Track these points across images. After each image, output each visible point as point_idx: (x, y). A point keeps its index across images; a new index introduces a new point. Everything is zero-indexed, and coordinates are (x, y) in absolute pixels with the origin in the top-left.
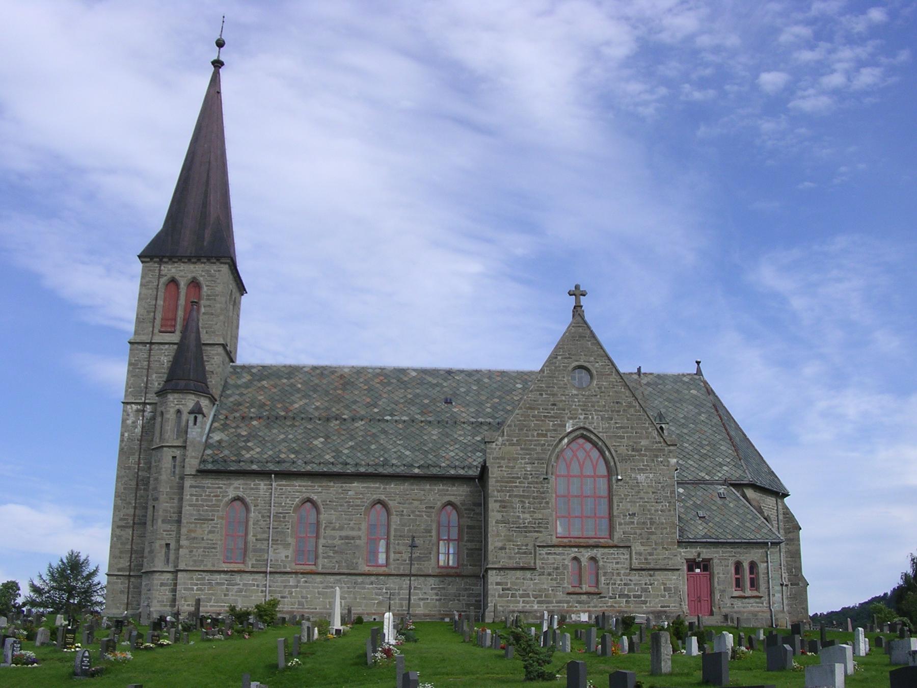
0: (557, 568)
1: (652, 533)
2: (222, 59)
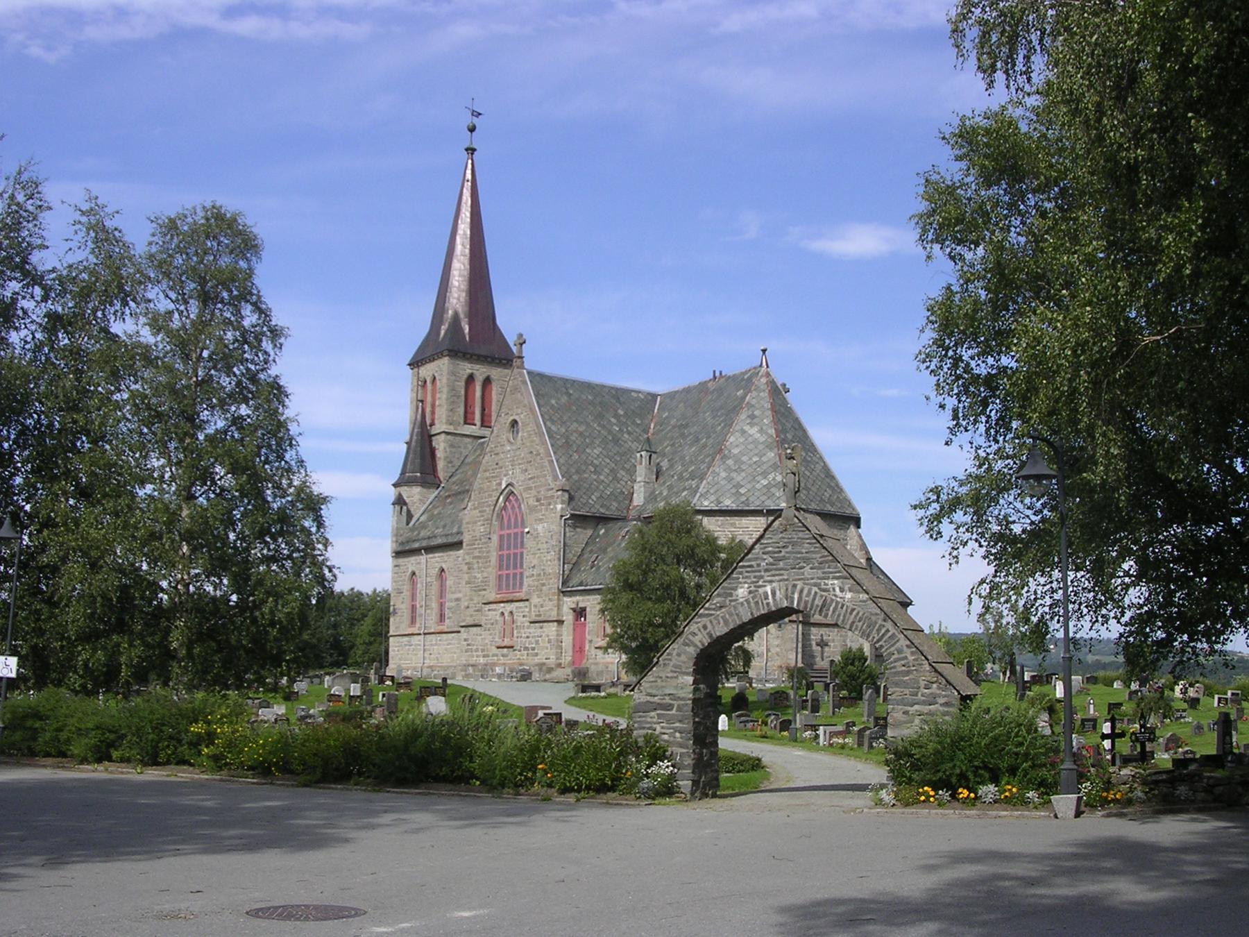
1: (543, 585)
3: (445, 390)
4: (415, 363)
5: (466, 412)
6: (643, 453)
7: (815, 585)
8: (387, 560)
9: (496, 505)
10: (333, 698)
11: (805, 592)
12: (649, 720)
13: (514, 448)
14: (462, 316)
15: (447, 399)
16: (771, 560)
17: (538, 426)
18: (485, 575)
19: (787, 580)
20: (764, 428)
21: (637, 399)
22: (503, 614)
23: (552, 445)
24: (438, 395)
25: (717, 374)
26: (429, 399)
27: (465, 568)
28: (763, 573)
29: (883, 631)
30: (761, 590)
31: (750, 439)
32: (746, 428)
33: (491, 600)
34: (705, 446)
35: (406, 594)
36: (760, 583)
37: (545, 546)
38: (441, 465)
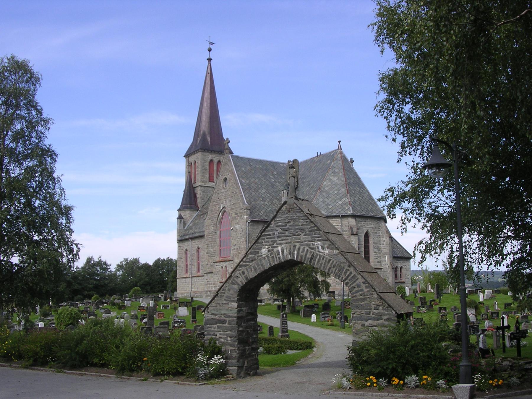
0: (218, 272)
1: (239, 253)
2: (211, 57)
3: (200, 167)
4: (187, 156)
5: (209, 176)
6: (284, 191)
7: (307, 245)
8: (176, 245)
9: (218, 217)
10: (141, 308)
11: (301, 250)
12: (213, 329)
13: (226, 190)
14: (207, 133)
15: (201, 171)
16: (281, 231)
17: (236, 180)
18: (214, 249)
19: (290, 242)
20: (340, 177)
21: (283, 167)
22: (222, 267)
23: (242, 189)
24: (197, 170)
25: (319, 154)
26: (193, 171)
27: (206, 246)
28: (276, 239)
29: (348, 273)
30: (275, 249)
31: (333, 183)
32: (332, 178)
33: (217, 261)
34: (312, 187)
35: (184, 259)
36: (275, 245)
37: (240, 235)
38: (199, 200)
